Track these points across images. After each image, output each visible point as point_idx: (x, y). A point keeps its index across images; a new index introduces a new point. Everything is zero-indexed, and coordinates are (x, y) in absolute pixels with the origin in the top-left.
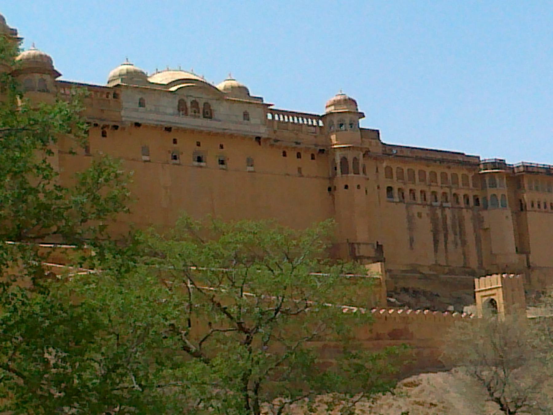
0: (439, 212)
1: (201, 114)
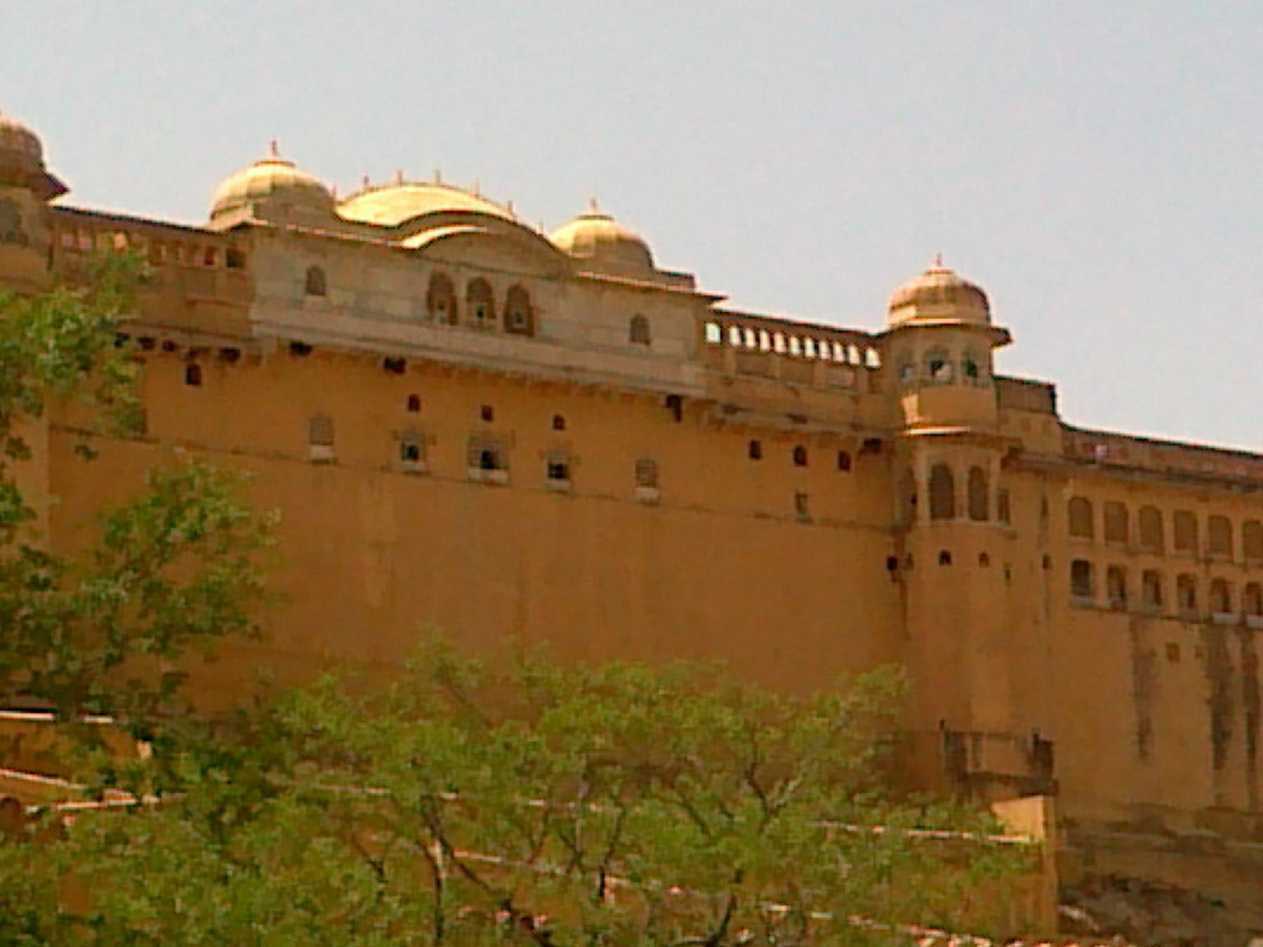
0: (1233, 644)
1: (499, 322)
